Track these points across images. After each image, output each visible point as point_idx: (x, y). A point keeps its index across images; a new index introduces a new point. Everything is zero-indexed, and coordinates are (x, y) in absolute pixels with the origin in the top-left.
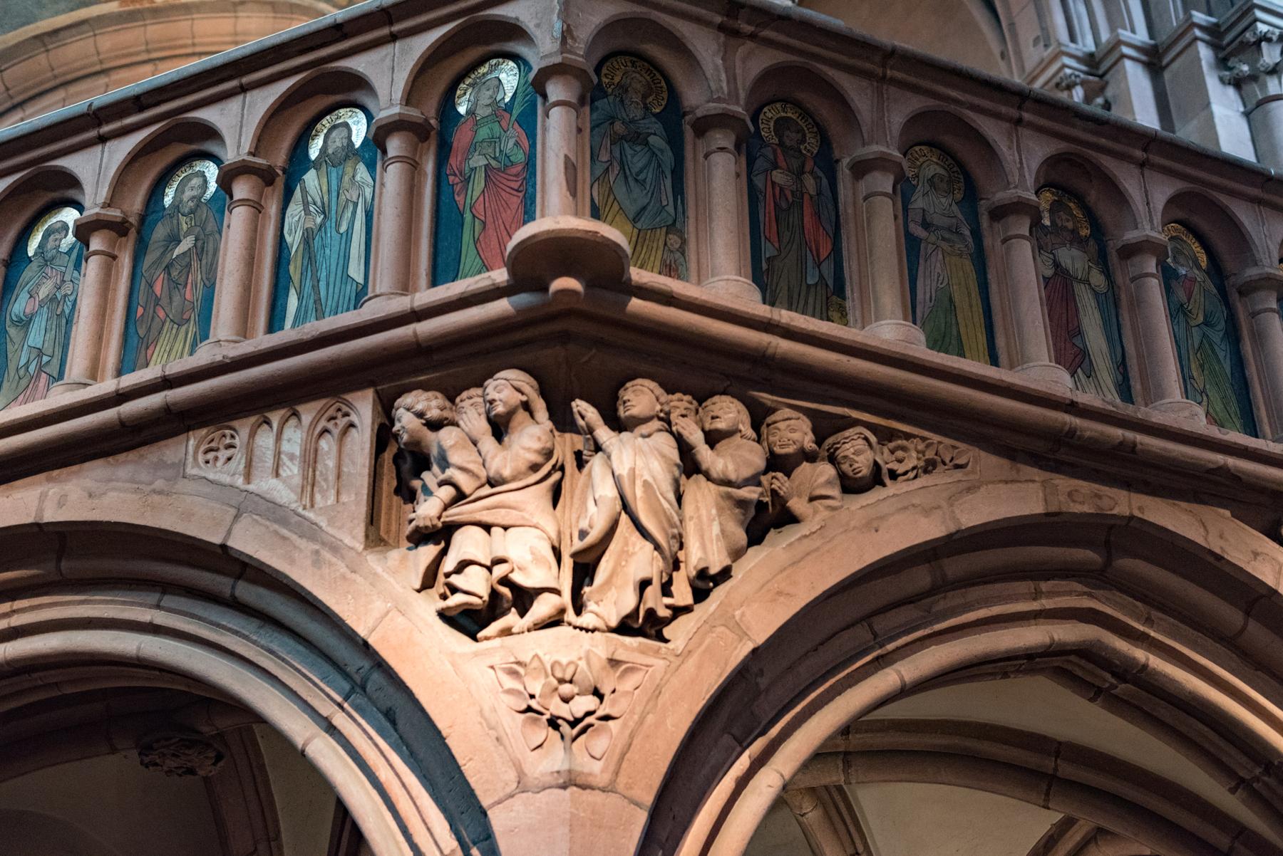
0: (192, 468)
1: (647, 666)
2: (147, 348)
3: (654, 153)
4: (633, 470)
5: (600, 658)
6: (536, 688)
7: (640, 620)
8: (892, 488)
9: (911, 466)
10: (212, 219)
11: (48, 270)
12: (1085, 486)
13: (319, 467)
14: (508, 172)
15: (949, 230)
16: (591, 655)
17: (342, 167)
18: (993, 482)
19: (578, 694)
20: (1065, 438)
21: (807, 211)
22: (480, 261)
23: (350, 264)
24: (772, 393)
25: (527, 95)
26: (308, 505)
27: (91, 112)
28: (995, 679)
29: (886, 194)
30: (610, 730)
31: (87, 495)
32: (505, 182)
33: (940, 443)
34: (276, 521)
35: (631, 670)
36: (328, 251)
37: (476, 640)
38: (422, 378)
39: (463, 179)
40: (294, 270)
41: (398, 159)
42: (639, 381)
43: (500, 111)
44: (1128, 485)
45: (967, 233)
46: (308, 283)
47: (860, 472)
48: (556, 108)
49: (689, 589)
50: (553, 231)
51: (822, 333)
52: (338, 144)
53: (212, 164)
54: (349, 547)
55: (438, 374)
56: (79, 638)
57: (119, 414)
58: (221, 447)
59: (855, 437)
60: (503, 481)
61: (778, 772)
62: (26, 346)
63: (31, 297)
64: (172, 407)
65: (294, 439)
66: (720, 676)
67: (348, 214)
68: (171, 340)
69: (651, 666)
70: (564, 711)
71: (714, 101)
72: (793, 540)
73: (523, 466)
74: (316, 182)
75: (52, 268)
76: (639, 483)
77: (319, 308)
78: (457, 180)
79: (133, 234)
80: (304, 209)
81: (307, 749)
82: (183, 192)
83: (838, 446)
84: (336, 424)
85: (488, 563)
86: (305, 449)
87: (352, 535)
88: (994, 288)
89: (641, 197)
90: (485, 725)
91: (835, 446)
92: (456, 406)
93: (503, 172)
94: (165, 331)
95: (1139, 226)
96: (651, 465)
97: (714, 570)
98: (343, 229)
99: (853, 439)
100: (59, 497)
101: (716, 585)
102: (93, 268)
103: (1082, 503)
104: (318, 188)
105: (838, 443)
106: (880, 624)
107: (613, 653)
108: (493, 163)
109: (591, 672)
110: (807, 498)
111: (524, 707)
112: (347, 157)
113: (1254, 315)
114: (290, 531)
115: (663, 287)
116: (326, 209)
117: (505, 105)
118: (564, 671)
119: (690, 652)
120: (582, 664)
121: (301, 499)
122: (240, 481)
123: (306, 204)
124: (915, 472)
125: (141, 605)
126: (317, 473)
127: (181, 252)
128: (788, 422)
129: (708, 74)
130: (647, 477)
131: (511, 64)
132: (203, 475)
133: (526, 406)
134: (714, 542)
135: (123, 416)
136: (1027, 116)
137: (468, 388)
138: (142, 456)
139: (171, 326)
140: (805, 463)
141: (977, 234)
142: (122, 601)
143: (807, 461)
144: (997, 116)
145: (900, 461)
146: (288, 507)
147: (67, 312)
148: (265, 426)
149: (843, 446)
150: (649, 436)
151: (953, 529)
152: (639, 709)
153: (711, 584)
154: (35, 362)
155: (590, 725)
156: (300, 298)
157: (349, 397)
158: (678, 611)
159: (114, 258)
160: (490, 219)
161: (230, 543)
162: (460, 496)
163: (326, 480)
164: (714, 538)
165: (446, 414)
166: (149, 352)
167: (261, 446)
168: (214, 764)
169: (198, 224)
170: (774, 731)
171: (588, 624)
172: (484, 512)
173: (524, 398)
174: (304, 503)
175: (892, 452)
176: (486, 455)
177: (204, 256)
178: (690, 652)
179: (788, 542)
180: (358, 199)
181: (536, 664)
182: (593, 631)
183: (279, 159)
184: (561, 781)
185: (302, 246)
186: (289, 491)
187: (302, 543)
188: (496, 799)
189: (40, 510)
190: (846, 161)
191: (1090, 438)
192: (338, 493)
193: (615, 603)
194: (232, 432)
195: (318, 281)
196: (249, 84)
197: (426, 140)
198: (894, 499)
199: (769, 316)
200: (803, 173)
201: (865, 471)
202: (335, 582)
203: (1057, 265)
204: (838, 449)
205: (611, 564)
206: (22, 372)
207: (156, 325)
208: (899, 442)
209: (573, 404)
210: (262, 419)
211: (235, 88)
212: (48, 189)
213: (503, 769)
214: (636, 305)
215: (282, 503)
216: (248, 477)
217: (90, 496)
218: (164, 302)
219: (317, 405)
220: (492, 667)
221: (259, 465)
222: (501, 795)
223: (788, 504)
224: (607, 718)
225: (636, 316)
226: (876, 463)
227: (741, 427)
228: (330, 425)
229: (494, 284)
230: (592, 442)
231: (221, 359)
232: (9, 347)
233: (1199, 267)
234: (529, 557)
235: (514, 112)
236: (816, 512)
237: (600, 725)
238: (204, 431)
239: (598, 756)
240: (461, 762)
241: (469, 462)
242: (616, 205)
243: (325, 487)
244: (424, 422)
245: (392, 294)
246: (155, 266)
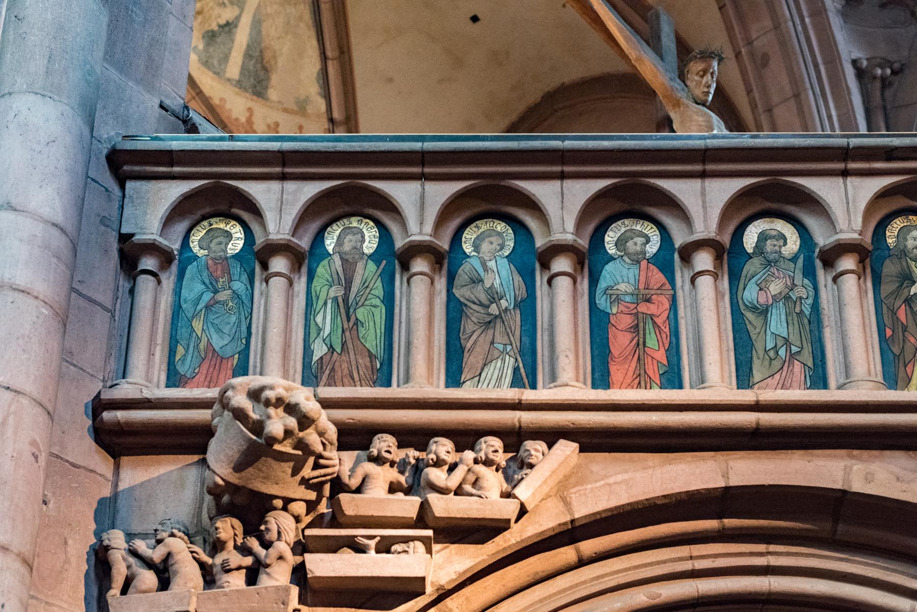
2: (906, 366)
11: (774, 270)
62: (768, 333)
63: (761, 289)
142: (892, 569)
147: (807, 313)
154: (784, 349)
166: (909, 369)
189: (847, 479)
206: (772, 354)
217: (898, 479)
232: (749, 327)
246: (894, 296)
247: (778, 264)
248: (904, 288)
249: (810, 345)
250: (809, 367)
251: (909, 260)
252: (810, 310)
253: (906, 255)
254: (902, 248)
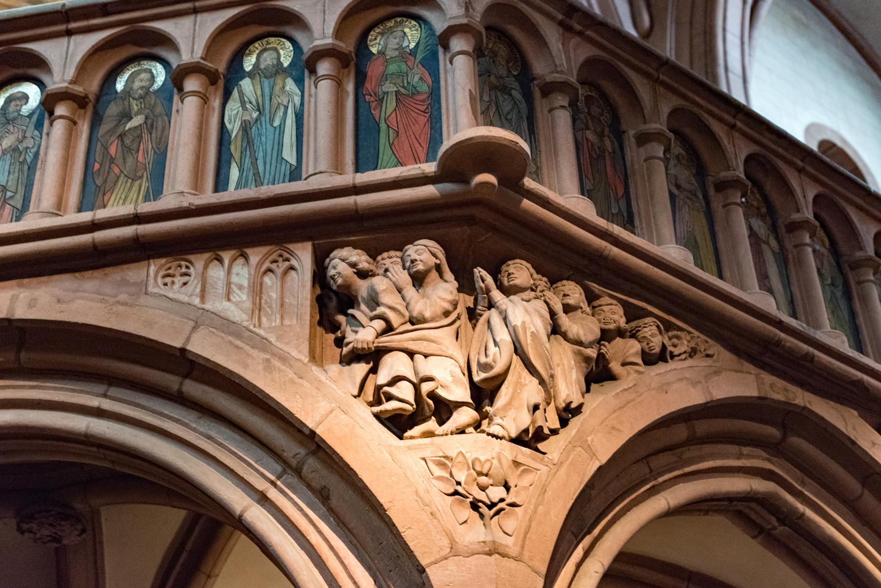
0: (154, 287)
1: (536, 469)
2: (104, 194)
3: (515, 102)
4: (524, 323)
5: (508, 459)
6: (461, 476)
7: (530, 435)
8: (672, 365)
9: (683, 350)
10: (160, 105)
11: (11, 127)
12: (780, 383)
13: (264, 297)
14: (415, 97)
15: (690, 192)
16: (502, 457)
17: (273, 79)
18: (728, 370)
19: (492, 485)
21: (608, 163)
22: (396, 159)
23: (284, 150)
24: (598, 284)
25: (428, 46)
26: (257, 325)
27: (63, 11)
28: (700, 515)
29: (659, 158)
30: (517, 514)
31: (55, 300)
32: (413, 105)
33: (698, 337)
34: (230, 334)
36: (263, 139)
37: (401, 438)
38: (353, 238)
39: (377, 99)
40: (235, 149)
41: (326, 77)
42: (518, 261)
43: (405, 55)
44: (802, 385)
45: (701, 197)
46: (248, 161)
47: (654, 349)
48: (460, 56)
49: (557, 417)
50: (487, 137)
51: (638, 245)
52: (269, 62)
53: (158, 64)
54: (296, 359)
55: (366, 237)
56: (31, 415)
57: (93, 239)
58: (177, 274)
59: (652, 324)
60: (425, 321)
61: (601, 562)
64: (141, 239)
65: (242, 274)
66: (581, 483)
67: (280, 113)
68: (127, 188)
69: (540, 470)
70: (481, 496)
71: (557, 72)
72: (618, 391)
73: (439, 312)
74: (251, 88)
75: (14, 126)
76: (529, 334)
77: (258, 179)
78: (372, 99)
79: (90, 108)
80: (241, 106)
81: (245, 515)
82: (133, 82)
83: (640, 329)
84: (278, 266)
85: (415, 381)
86: (254, 282)
87: (299, 352)
88: (720, 236)
90: (420, 502)
91: (637, 329)
92: (378, 262)
93: (411, 98)
94: (120, 183)
95: (801, 210)
96: (535, 322)
97: (573, 406)
98: (276, 123)
99: (651, 325)
100: (29, 299)
101: (573, 417)
102: (59, 128)
103: (778, 393)
104: (253, 92)
105: (640, 327)
106: (656, 462)
107: (516, 457)
108: (403, 90)
109: (503, 469)
110: (620, 363)
111: (451, 491)
112: (277, 73)
113: (859, 283)
114: (244, 342)
115: (543, 193)
116: (261, 108)
117: (410, 50)
118: (482, 466)
119: (562, 462)
120: (495, 462)
121: (252, 319)
122: (197, 301)
123: (243, 104)
124: (685, 354)
125: (88, 393)
126: (263, 301)
127: (132, 126)
128: (610, 307)
129: (554, 54)
130: (533, 330)
131: (413, 23)
132: (164, 293)
133: (438, 268)
134: (574, 384)
135: (96, 241)
136: (739, 124)
137: (388, 251)
138: (106, 275)
139: (125, 180)
140: (618, 338)
143: (619, 337)
144: (720, 120)
145: (675, 346)
146: (240, 325)
147: (29, 160)
148: (216, 262)
149: (644, 329)
150: (528, 301)
151: (709, 400)
152: (533, 501)
153: (570, 415)
155: (502, 510)
156: (241, 170)
157: (291, 246)
159: (75, 123)
160: (402, 131)
161: (189, 348)
162: (389, 329)
163: (270, 307)
164: (574, 382)
165: (372, 267)
166: (106, 198)
167: (213, 277)
168: (79, 535)
169: (147, 106)
170: (596, 531)
171: (498, 432)
172: (410, 342)
173: (438, 262)
174: (254, 322)
175: (670, 339)
176: (410, 300)
177: (154, 131)
178: (562, 462)
179: (616, 393)
180: (288, 103)
181: (460, 459)
182: (501, 438)
183: (221, 66)
184: (487, 549)
185: (241, 133)
186: (241, 312)
187: (255, 353)
188: (433, 559)
189: (11, 308)
190: (632, 133)
191: (789, 348)
192: (282, 318)
193: (514, 419)
194: (187, 264)
195: (256, 159)
196: (200, 8)
197: (346, 68)
198: (674, 372)
199: (607, 228)
200: (604, 136)
201: (657, 350)
202: (285, 385)
204: (639, 331)
205: (511, 390)
207: (112, 177)
208: (676, 332)
209: (475, 270)
210: (214, 256)
211: (190, 9)
212: (14, 67)
213: (438, 537)
214: (527, 203)
215: (235, 320)
216: (203, 297)
217: (59, 301)
218: (119, 161)
219: (264, 250)
220: (424, 459)
221: (211, 291)
222: (438, 557)
223: (610, 366)
225: (526, 212)
226: (663, 344)
227: (582, 305)
228: (274, 266)
229: (423, 173)
230: (486, 301)
231: (188, 205)
233: (825, 246)
234: (450, 379)
235: (417, 56)
236: (628, 374)
237: (510, 509)
238: (163, 261)
239: (510, 533)
240: (401, 529)
241: (397, 304)
243: (270, 312)
244: (355, 271)
245: (333, 172)
246: (110, 134)
247: (16, 121)
248: (121, 125)
249: (24, 188)
250: (17, 209)
251: (131, 99)
252: (32, 157)
253: (130, 96)
254: (128, 90)
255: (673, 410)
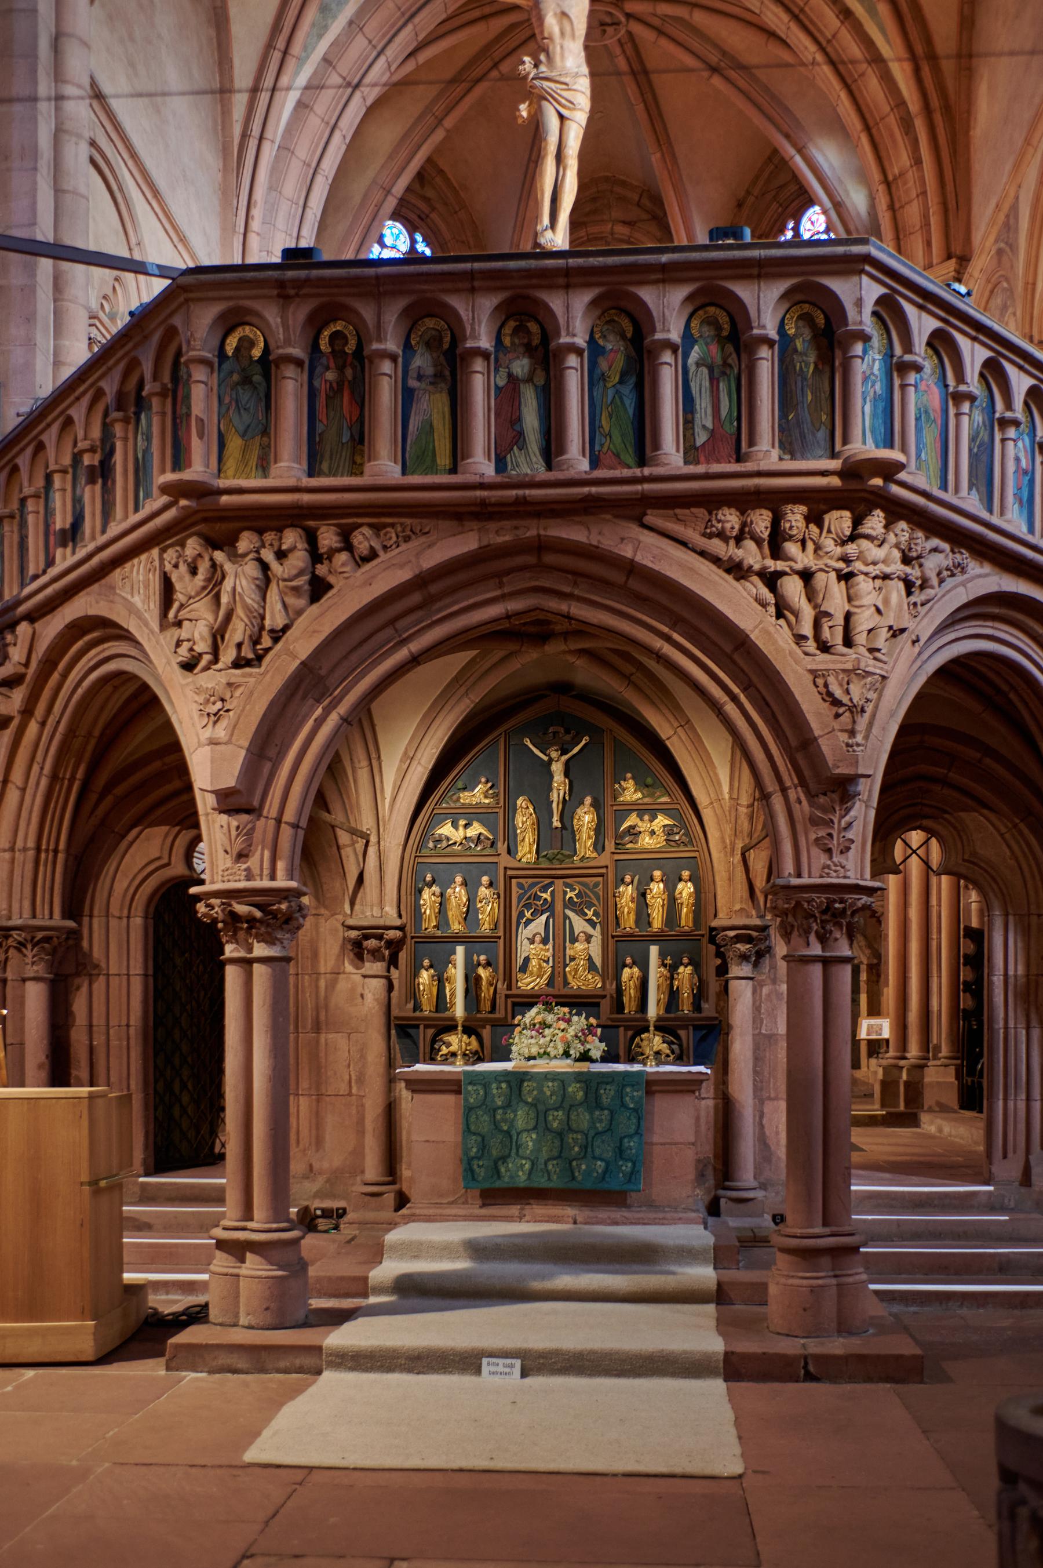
3: (256, 388)
20: (483, 503)
35: (239, 686)
45: (447, 373)
89: (246, 418)
133: (200, 555)
141: (453, 374)
158: (267, 650)
203: (510, 375)
224: (228, 711)
226: (371, 546)
242: (233, 430)
255: (376, 596)
